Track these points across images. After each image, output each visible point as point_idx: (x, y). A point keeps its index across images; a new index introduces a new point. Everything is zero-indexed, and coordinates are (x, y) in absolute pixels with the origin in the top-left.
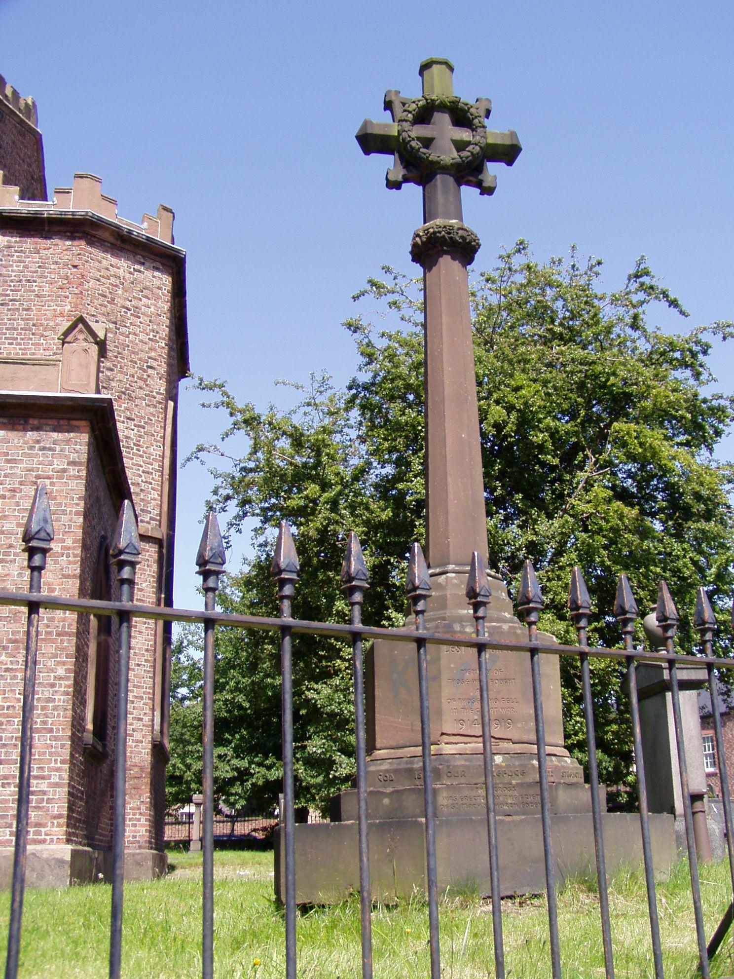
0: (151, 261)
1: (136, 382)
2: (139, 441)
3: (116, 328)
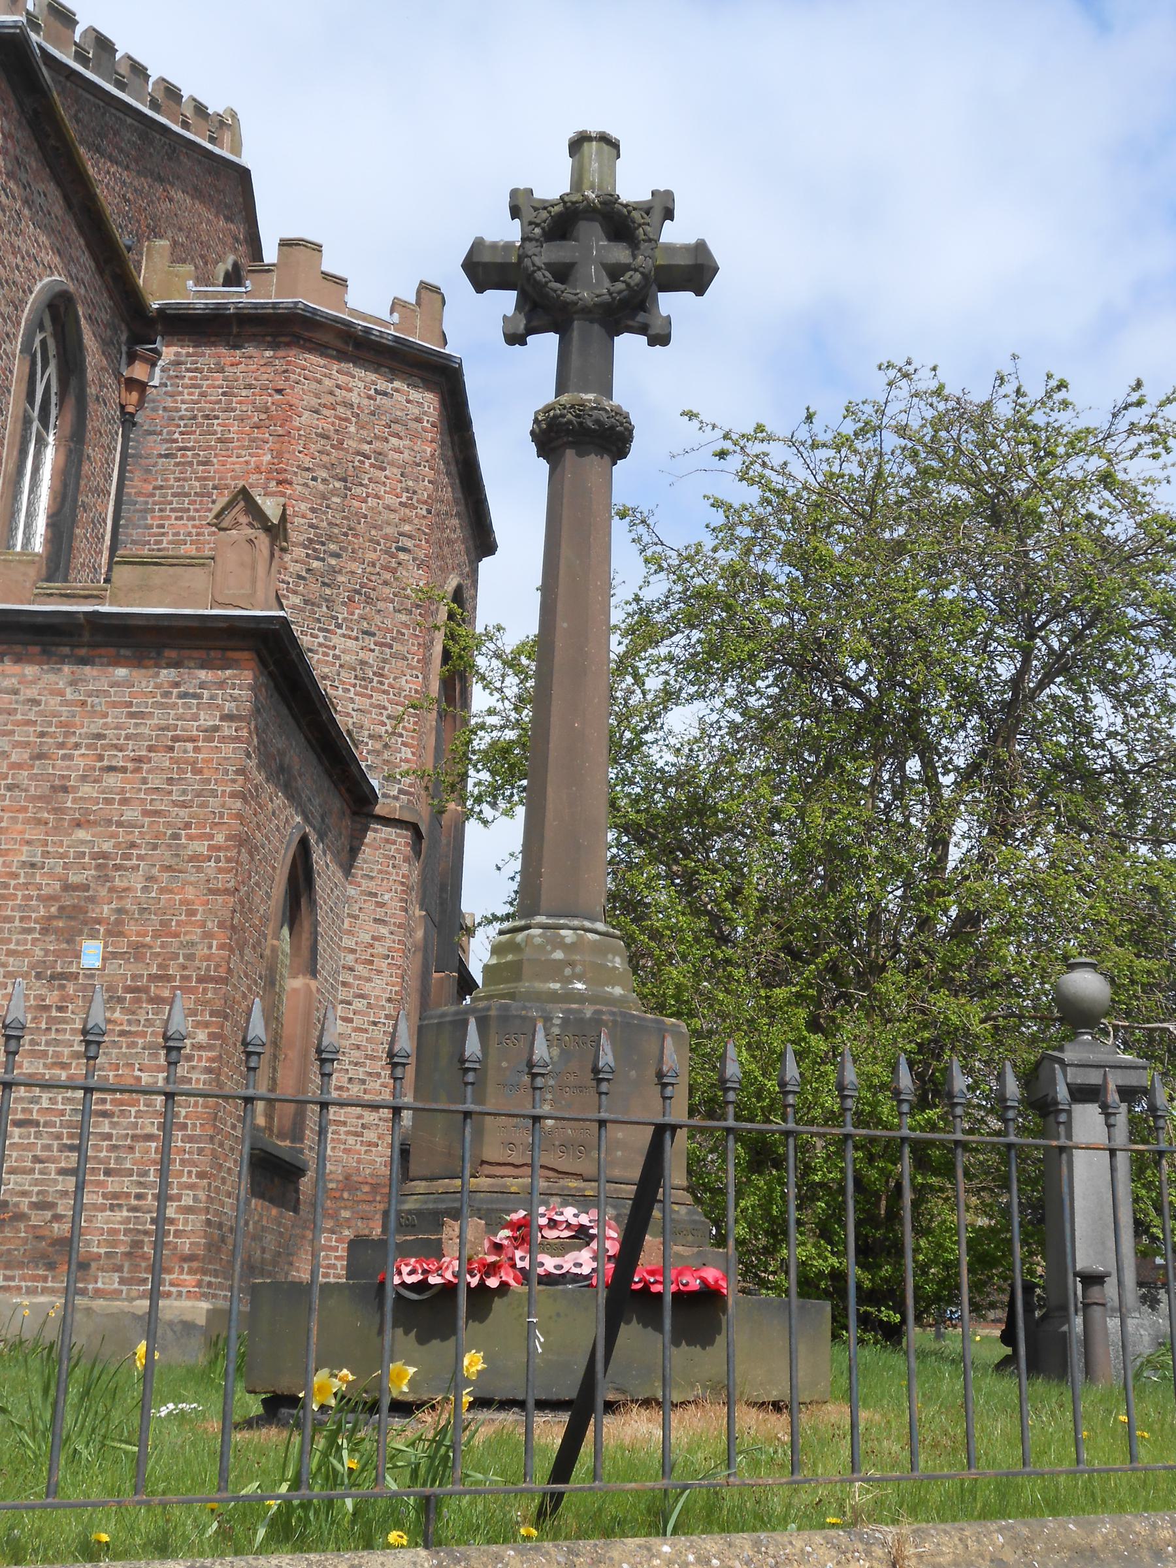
0: (405, 376)
1: (378, 574)
3: (346, 488)
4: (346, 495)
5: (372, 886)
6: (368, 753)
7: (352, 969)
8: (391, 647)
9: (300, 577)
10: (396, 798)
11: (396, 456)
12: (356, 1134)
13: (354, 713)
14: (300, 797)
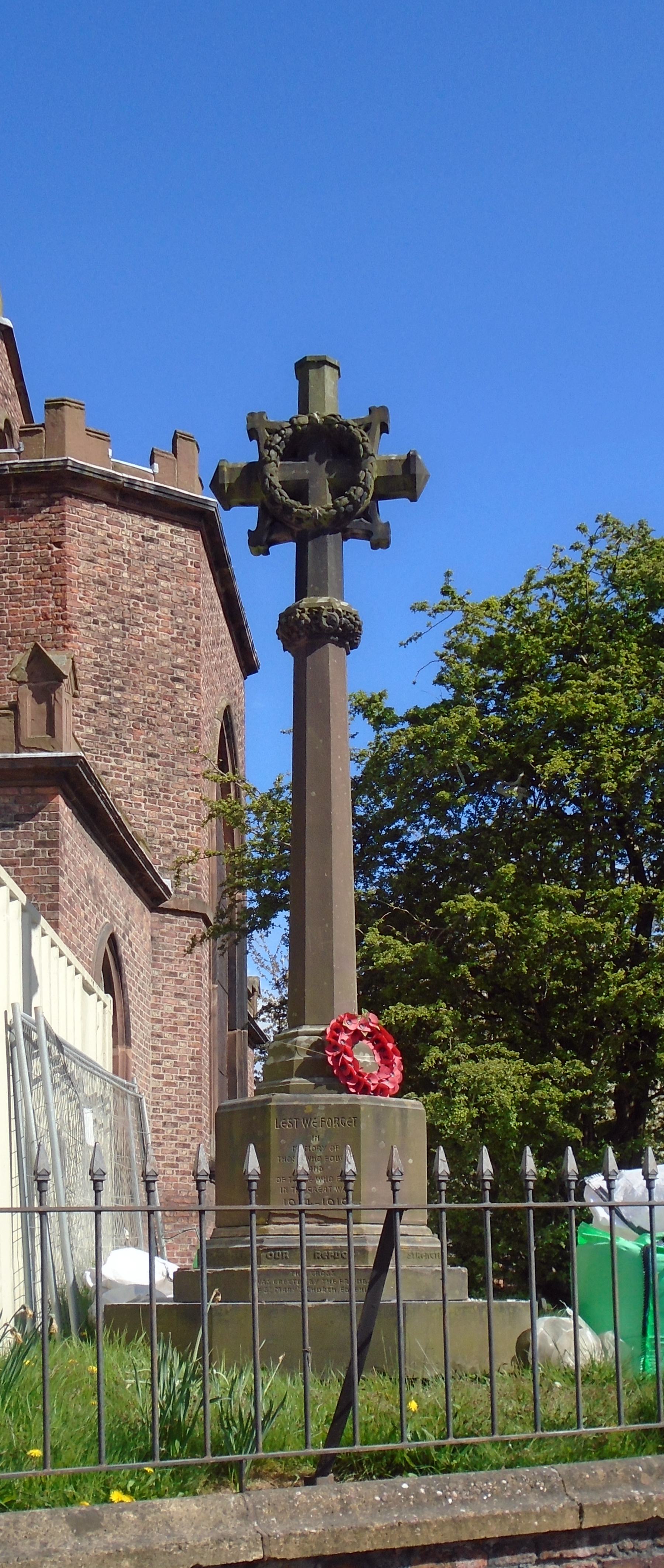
1: (158, 703)
2: (167, 785)
3: (124, 628)
4: (125, 635)
5: (171, 967)
6: (160, 858)
7: (159, 1036)
8: (173, 766)
9: (91, 710)
10: (187, 894)
11: (166, 597)
12: (172, 1166)
13: (146, 824)
14: (107, 901)
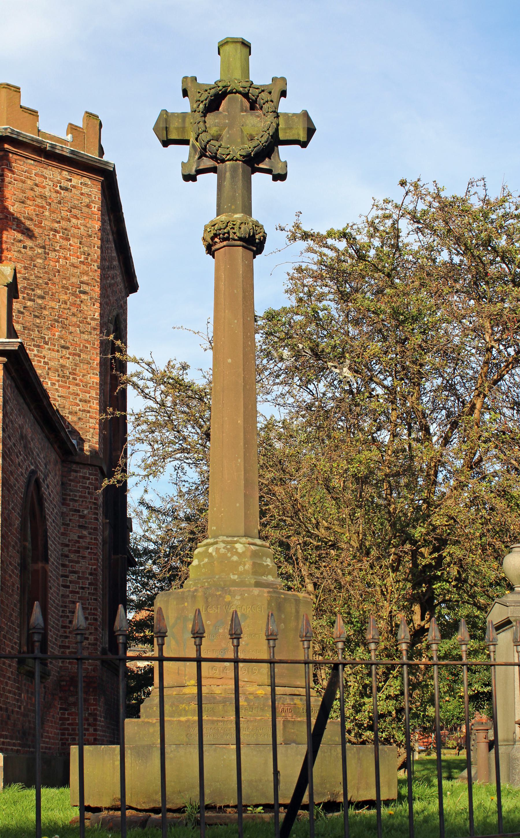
0: (79, 177)
1: (69, 309)
2: (75, 369)
3: (45, 253)
8: (79, 356)
11: (76, 231)
13: (59, 399)
14: (33, 454)
